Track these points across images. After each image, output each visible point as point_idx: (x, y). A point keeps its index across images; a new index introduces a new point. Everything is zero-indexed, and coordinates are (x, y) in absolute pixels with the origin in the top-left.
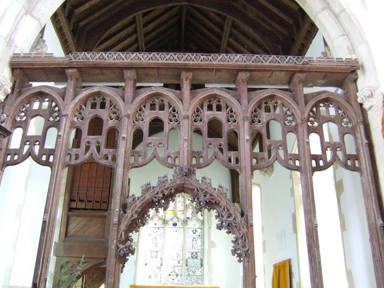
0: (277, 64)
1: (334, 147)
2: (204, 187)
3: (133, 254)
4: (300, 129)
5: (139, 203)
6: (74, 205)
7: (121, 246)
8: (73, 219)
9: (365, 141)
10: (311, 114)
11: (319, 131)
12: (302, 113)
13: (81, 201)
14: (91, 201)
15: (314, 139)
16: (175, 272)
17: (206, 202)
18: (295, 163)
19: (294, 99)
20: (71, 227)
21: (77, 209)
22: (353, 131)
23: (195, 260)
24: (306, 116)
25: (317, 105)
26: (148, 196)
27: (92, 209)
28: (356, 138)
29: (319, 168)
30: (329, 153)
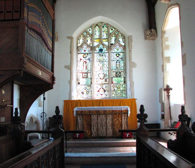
16: (103, 88)
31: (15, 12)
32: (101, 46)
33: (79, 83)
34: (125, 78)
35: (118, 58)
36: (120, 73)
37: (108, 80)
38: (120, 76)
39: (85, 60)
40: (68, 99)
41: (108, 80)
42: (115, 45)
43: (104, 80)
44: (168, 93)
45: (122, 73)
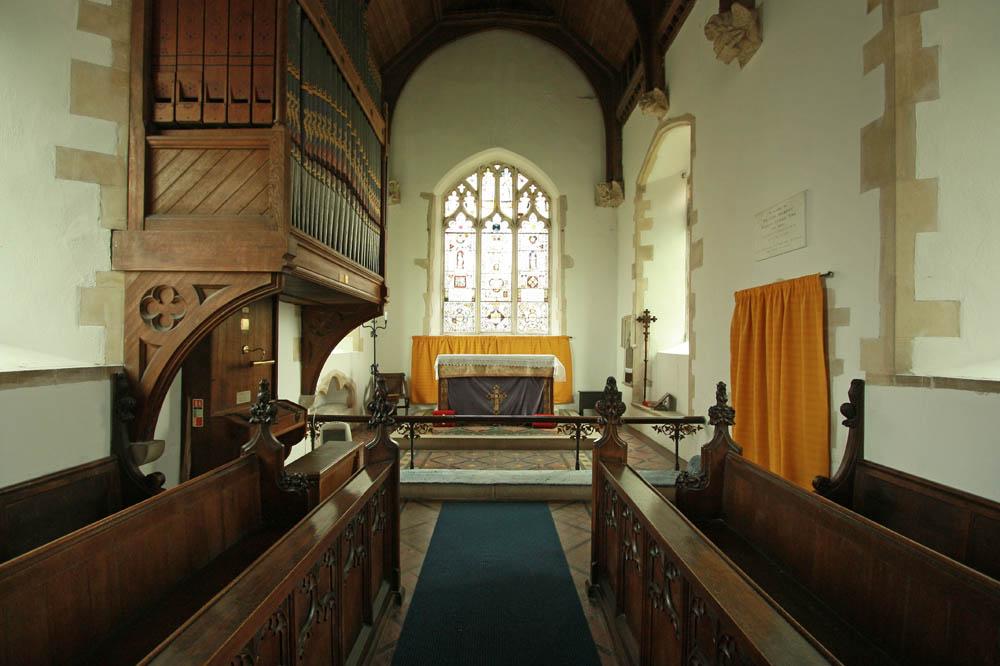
6: (164, 114)
8: (163, 158)
13: (184, 99)
14: (221, 101)
20: (162, 183)
21: (177, 125)
23: (536, 290)
27: (226, 126)
31: (258, 101)
32: (497, 219)
33: (446, 300)
34: (549, 290)
35: (533, 247)
37: (509, 294)
39: (460, 249)
40: (420, 334)
41: (509, 294)
42: (527, 216)
43: (501, 292)
44: (647, 327)
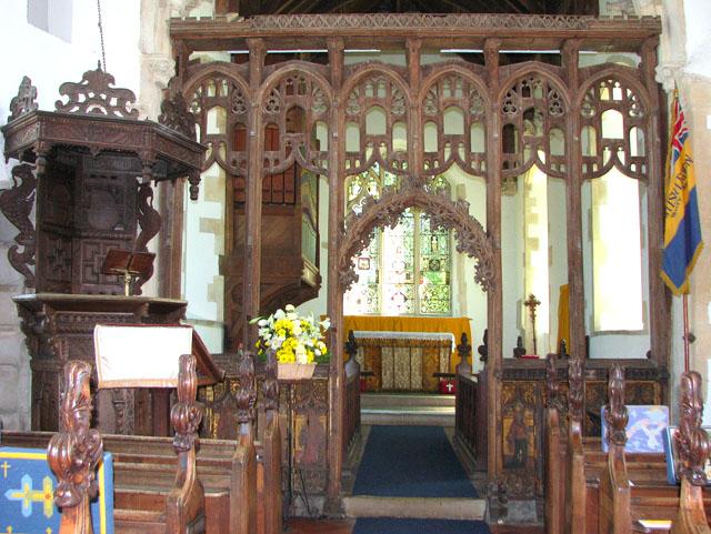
0: (539, 29)
1: (614, 145)
2: (439, 201)
3: (356, 281)
4: (569, 121)
5: (360, 222)
7: (343, 273)
9: (658, 139)
10: (587, 98)
11: (596, 123)
12: (573, 99)
15: (589, 135)
17: (447, 217)
18: (559, 168)
19: (564, 77)
22: (642, 124)
24: (578, 103)
25: (597, 86)
26: (371, 213)
28: (646, 132)
29: (592, 175)
30: (607, 154)
34: (448, 273)
36: (438, 261)
38: (438, 270)
45: (442, 263)
